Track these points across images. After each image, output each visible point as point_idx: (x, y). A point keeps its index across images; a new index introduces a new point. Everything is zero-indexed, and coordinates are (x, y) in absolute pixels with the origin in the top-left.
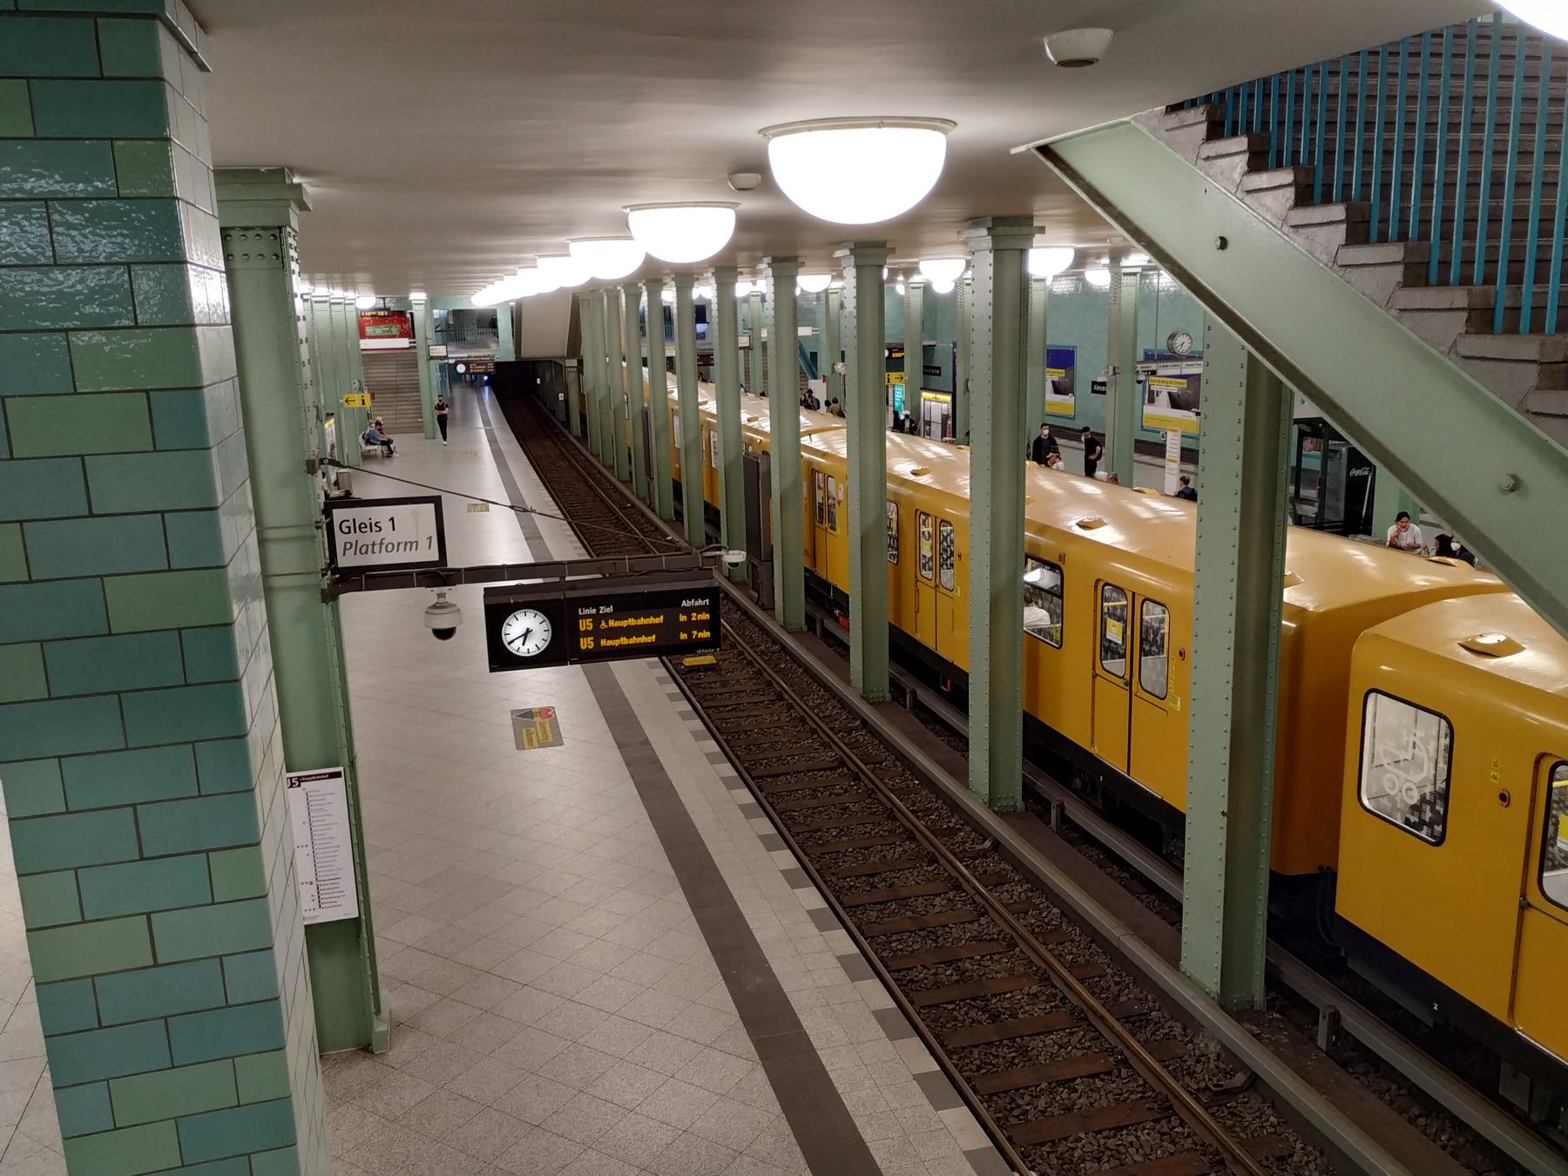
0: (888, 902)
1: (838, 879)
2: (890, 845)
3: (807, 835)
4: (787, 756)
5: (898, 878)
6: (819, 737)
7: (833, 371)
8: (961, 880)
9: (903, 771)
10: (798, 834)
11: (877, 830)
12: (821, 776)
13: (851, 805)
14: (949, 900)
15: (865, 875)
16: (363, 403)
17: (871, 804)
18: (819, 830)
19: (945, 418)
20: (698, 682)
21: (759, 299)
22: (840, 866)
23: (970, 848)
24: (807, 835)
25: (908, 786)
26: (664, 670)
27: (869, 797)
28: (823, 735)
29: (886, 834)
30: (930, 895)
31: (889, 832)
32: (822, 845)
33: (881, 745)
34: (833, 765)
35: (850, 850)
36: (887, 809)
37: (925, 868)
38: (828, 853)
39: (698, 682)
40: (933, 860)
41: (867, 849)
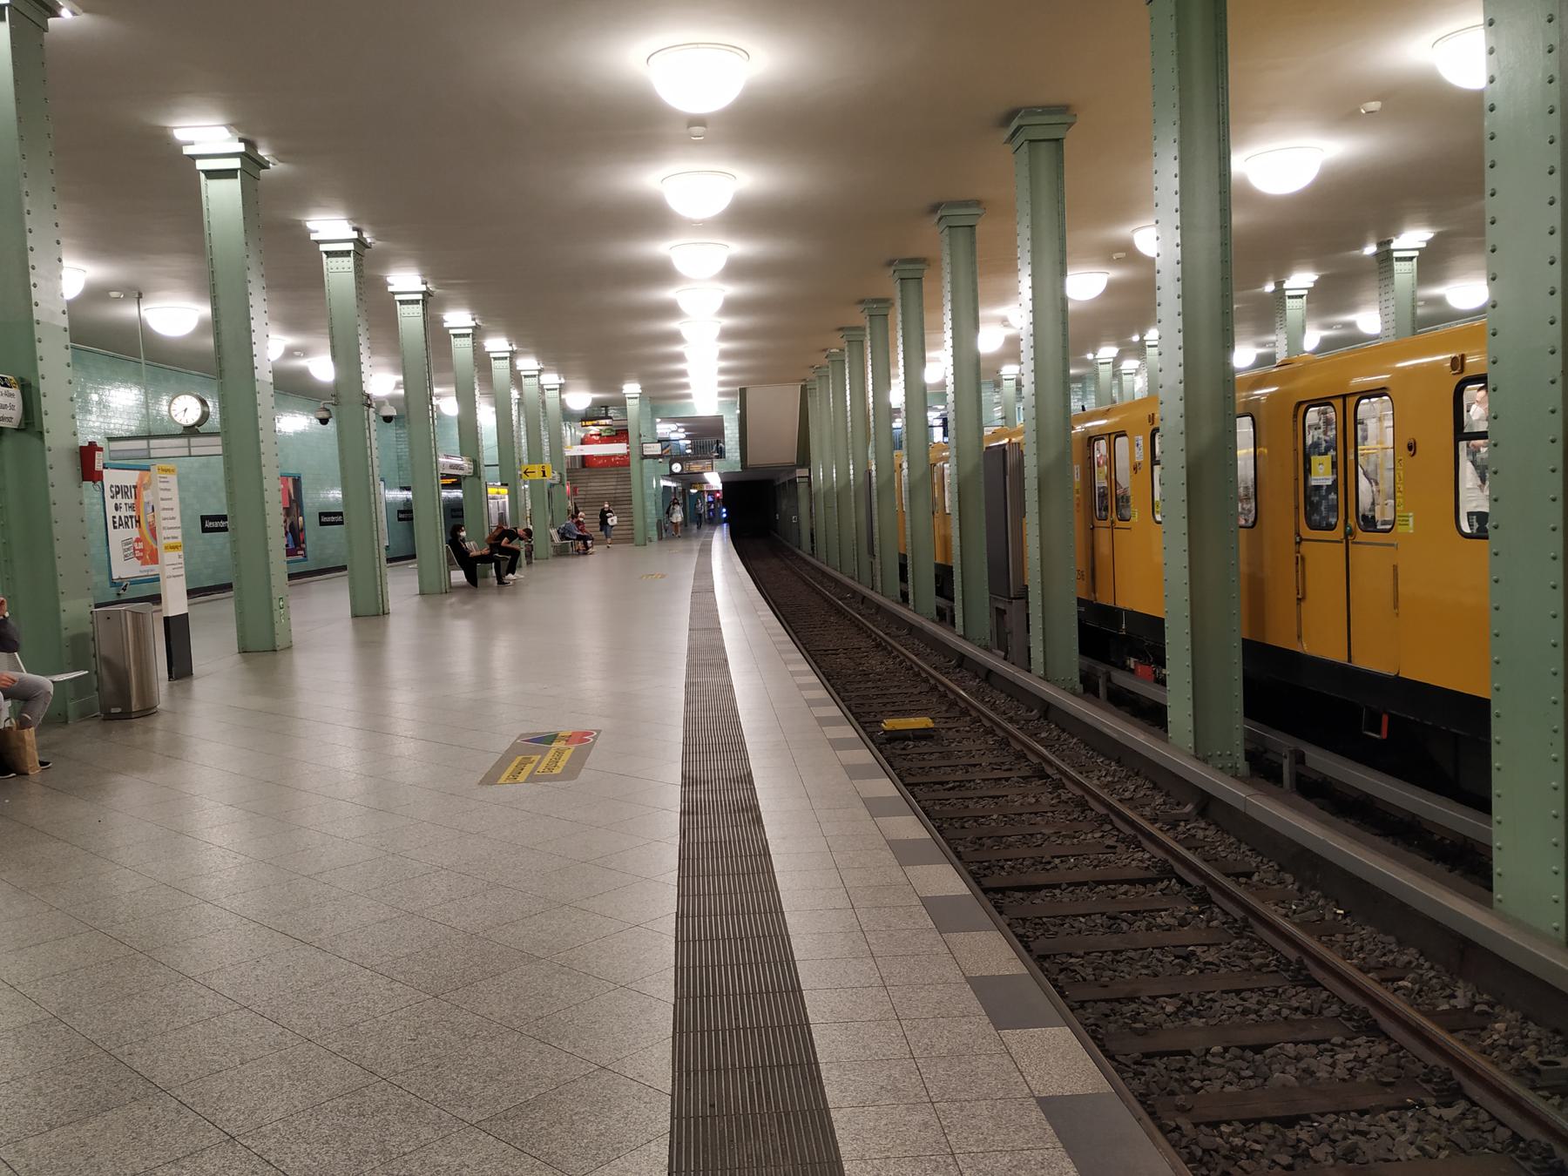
1: (1196, 1125)
2: (1317, 1043)
4: (1053, 857)
5: (1364, 1134)
6: (1114, 828)
9: (1300, 890)
10: (1082, 1004)
12: (1125, 893)
13: (1199, 950)
15: (1271, 1120)
16: (544, 475)
18: (1132, 1000)
20: (904, 752)
21: (1013, 382)
22: (1197, 1090)
23: (1541, 1062)
24: (1104, 1007)
26: (800, 654)
27: (1239, 936)
29: (1299, 1016)
31: (1305, 1012)
32: (1143, 1033)
33: (1243, 846)
34: (1149, 874)
35: (1216, 1049)
37: (1434, 1111)
38: (1161, 1055)
39: (904, 752)
40: (1450, 1094)
41: (1258, 1049)
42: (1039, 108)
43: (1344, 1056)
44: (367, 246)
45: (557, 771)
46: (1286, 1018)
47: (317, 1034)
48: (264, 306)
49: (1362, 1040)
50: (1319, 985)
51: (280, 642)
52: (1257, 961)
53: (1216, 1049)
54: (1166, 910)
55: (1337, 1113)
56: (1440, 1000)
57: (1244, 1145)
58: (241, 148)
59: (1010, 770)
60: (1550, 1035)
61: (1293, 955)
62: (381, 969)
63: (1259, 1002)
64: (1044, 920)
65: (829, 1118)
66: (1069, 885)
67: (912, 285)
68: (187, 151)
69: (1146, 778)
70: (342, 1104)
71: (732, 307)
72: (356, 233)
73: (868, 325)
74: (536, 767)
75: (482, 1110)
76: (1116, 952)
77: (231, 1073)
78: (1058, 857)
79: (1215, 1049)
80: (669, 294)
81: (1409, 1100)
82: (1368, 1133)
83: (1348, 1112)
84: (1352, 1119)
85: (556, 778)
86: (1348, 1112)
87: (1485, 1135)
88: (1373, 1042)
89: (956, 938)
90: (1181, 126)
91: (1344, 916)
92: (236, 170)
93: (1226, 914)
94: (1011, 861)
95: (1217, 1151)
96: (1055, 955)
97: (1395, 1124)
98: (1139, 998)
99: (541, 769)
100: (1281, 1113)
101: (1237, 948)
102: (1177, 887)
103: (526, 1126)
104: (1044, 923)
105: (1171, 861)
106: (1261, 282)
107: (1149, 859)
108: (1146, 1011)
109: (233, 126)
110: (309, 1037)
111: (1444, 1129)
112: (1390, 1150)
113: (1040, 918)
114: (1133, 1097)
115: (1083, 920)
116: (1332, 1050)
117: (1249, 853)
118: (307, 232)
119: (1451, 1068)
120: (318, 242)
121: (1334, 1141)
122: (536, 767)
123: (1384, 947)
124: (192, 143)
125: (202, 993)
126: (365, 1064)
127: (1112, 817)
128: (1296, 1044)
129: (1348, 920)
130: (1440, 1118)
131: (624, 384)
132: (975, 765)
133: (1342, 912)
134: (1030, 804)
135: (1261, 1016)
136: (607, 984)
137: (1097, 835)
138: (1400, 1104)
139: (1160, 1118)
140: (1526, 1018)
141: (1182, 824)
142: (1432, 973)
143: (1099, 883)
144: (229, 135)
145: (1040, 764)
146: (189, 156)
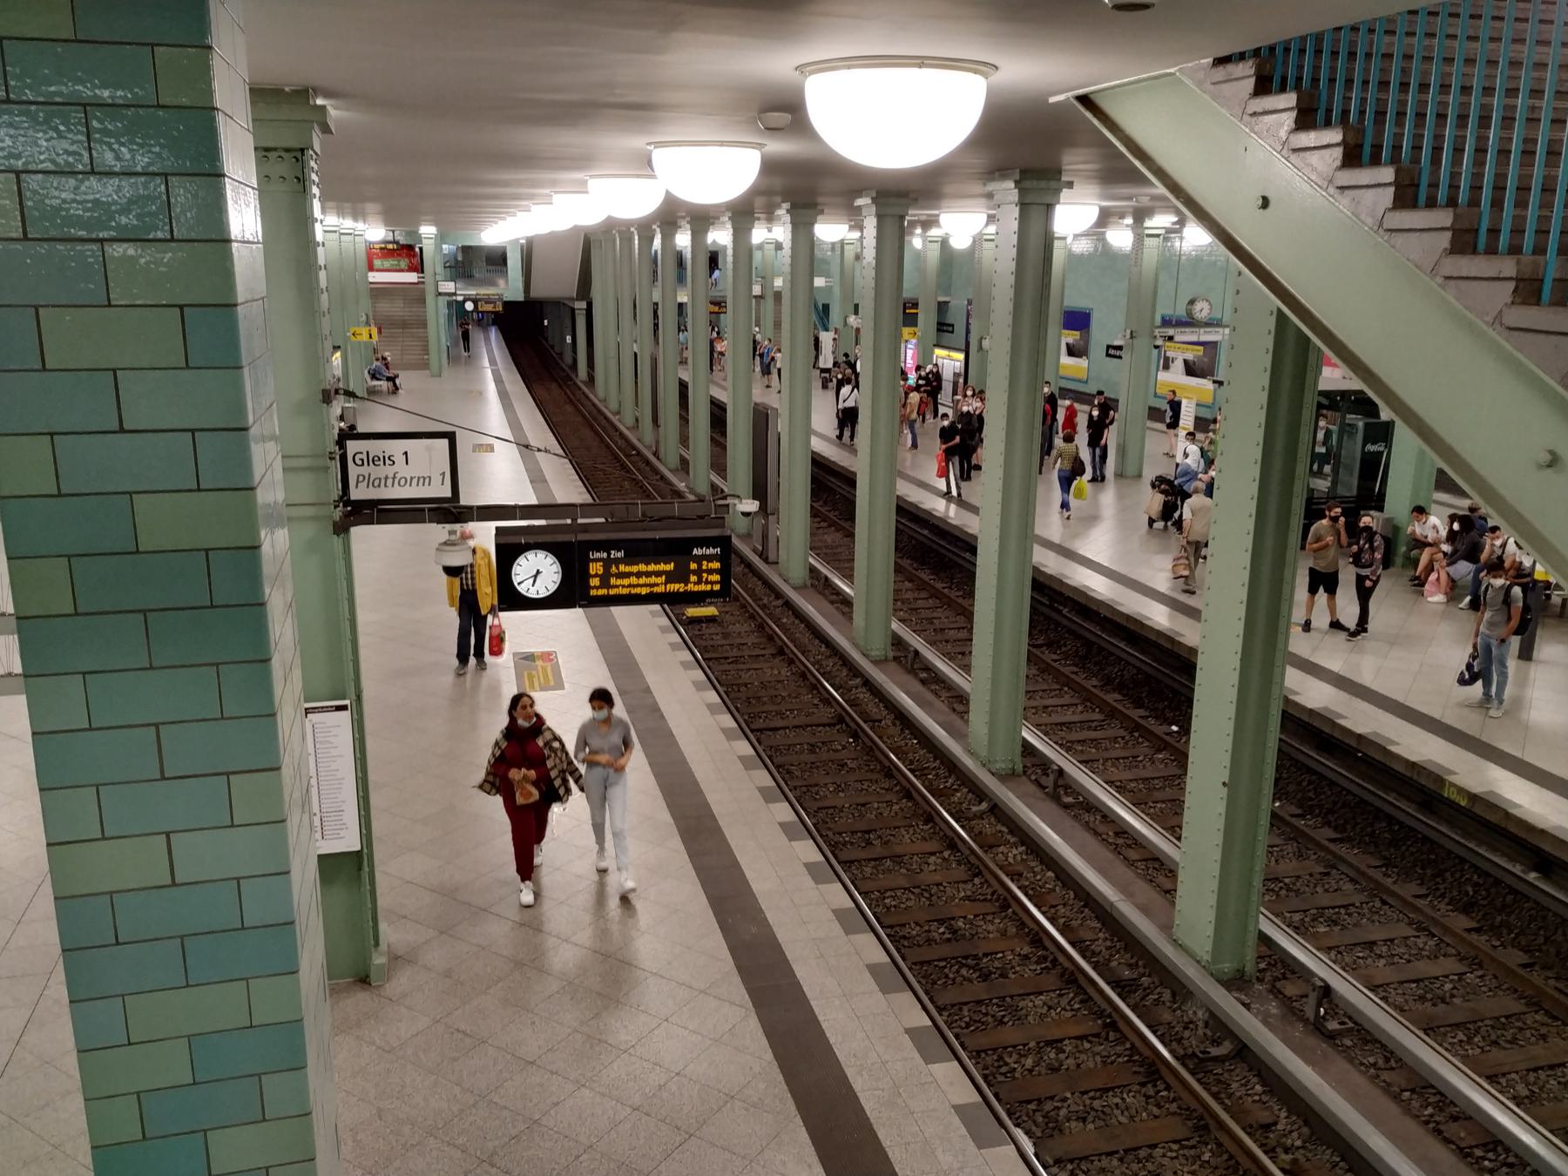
0: (883, 858)
3: (804, 789)
5: (894, 836)
6: (819, 692)
7: (845, 323)
8: (956, 839)
14: (944, 859)
18: (817, 785)
19: (956, 375)
21: (773, 246)
24: (804, 789)
25: (907, 744)
27: (867, 754)
29: (884, 791)
36: (885, 767)
38: (825, 808)
41: (863, 805)
49: (904, 801)
53: (847, 805)
59: (764, 649)
76: (812, 763)
89: (752, 772)
100: (863, 829)
131: (420, 225)
137: (810, 696)
140: (969, 792)
143: (807, 726)
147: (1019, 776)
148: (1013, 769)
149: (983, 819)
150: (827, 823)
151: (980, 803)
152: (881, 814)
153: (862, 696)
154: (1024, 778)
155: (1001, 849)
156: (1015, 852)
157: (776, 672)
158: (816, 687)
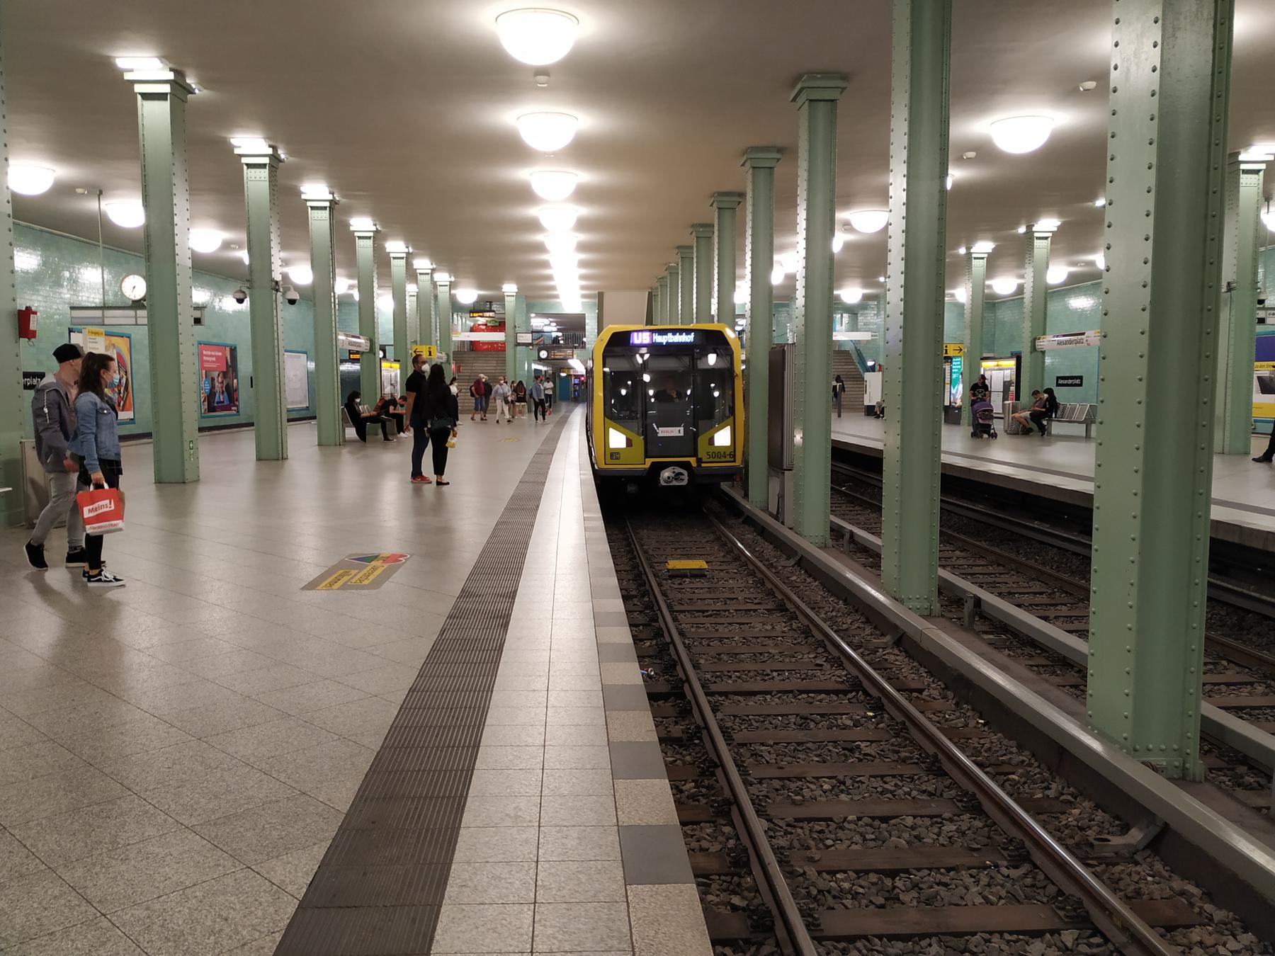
0: (923, 936)
1: (819, 873)
2: (931, 817)
3: (776, 784)
4: (772, 671)
5: (946, 885)
6: (826, 651)
8: (1087, 903)
11: (907, 789)
12: (820, 701)
13: (863, 745)
15: (877, 872)
16: (430, 355)
17: (899, 745)
18: (800, 779)
19: (1006, 385)
20: (680, 586)
22: (828, 847)
24: (776, 784)
25: (966, 725)
27: (897, 736)
28: (830, 648)
29: (924, 797)
30: (1018, 933)
34: (842, 687)
37: (1005, 871)
38: (809, 820)
39: (680, 586)
41: (885, 819)
42: (819, 73)
43: (949, 828)
44: (280, 161)
45: (366, 582)
46: (914, 798)
47: (98, 760)
48: (187, 205)
49: (966, 817)
50: (947, 774)
51: (189, 476)
52: (903, 754)
54: (847, 714)
55: (930, 869)
56: (1038, 791)
57: (851, 888)
58: (171, 76)
60: (1112, 820)
61: (931, 750)
62: (167, 718)
63: (896, 785)
64: (750, 717)
65: (458, 833)
66: (779, 692)
67: (727, 214)
68: (127, 76)
69: (862, 614)
70: (96, 809)
71: (584, 225)
72: (271, 149)
73: (695, 245)
74: (351, 578)
75: (199, 818)
76: (799, 744)
77: (22, 784)
78: (776, 671)
79: (850, 818)
80: (532, 212)
81: (988, 862)
82: (949, 885)
83: (938, 869)
84: (941, 874)
85: (363, 587)
86: (938, 869)
87: (1039, 891)
88: (974, 819)
90: (911, 93)
91: (984, 725)
92: (167, 94)
93: (893, 719)
94: (738, 672)
95: (829, 892)
96: (751, 744)
97: (973, 880)
98: (805, 778)
99: (354, 580)
101: (893, 745)
102: (862, 698)
103: (228, 830)
104: (750, 720)
105: (861, 677)
106: (1017, 224)
107: (845, 676)
108: (808, 788)
109: (164, 58)
110: (92, 763)
111: (1008, 885)
112: (962, 898)
113: (748, 716)
114: (769, 846)
115: (780, 718)
116: (941, 823)
117: (925, 675)
118: (231, 148)
119: (1024, 839)
120: (241, 156)
121: (921, 889)
122: (351, 578)
123: (1006, 750)
124: (131, 71)
125: (24, 729)
126: (125, 783)
127: (826, 642)
128: (915, 817)
129: (986, 729)
130: (1008, 876)
132: (733, 599)
133: (982, 721)
134: (767, 630)
135: (894, 796)
136: (334, 735)
137: (812, 656)
138: (981, 865)
139: (792, 866)
141: (880, 650)
142: (1037, 770)
143: (801, 692)
144: (161, 65)
145: (783, 600)
146: (128, 81)
147: (1194, 781)
148: (1184, 769)
149: (1137, 863)
150: (808, 848)
151: (1125, 829)
152: (919, 838)
153: (892, 658)
154: (1208, 786)
155: (1196, 935)
156: (1233, 945)
157: (769, 627)
158: (824, 644)
